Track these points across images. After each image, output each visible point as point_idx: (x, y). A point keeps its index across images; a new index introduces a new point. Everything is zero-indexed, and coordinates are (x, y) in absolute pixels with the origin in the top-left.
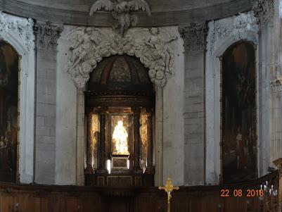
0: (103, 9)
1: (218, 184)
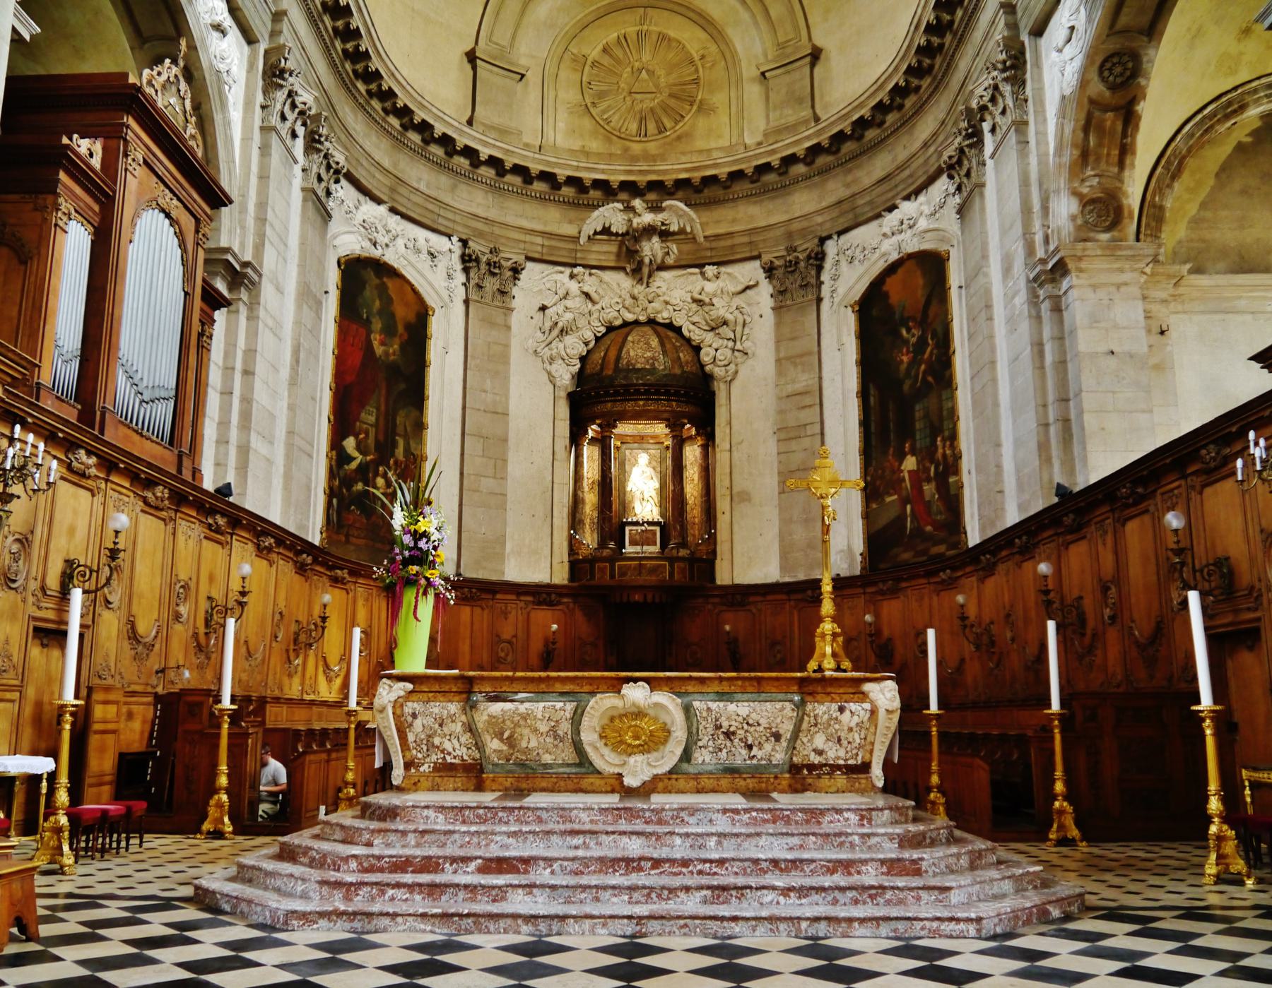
0: (606, 231)
1: (858, 573)
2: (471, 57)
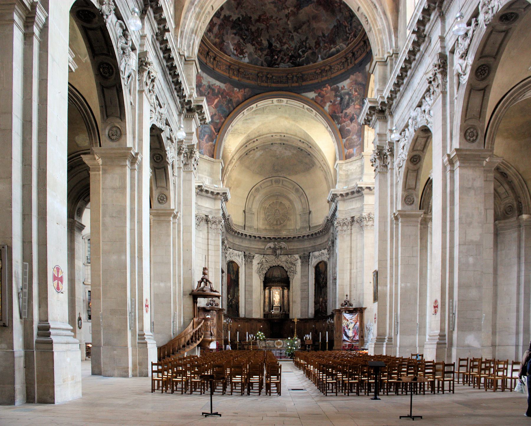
2: (244, 211)
